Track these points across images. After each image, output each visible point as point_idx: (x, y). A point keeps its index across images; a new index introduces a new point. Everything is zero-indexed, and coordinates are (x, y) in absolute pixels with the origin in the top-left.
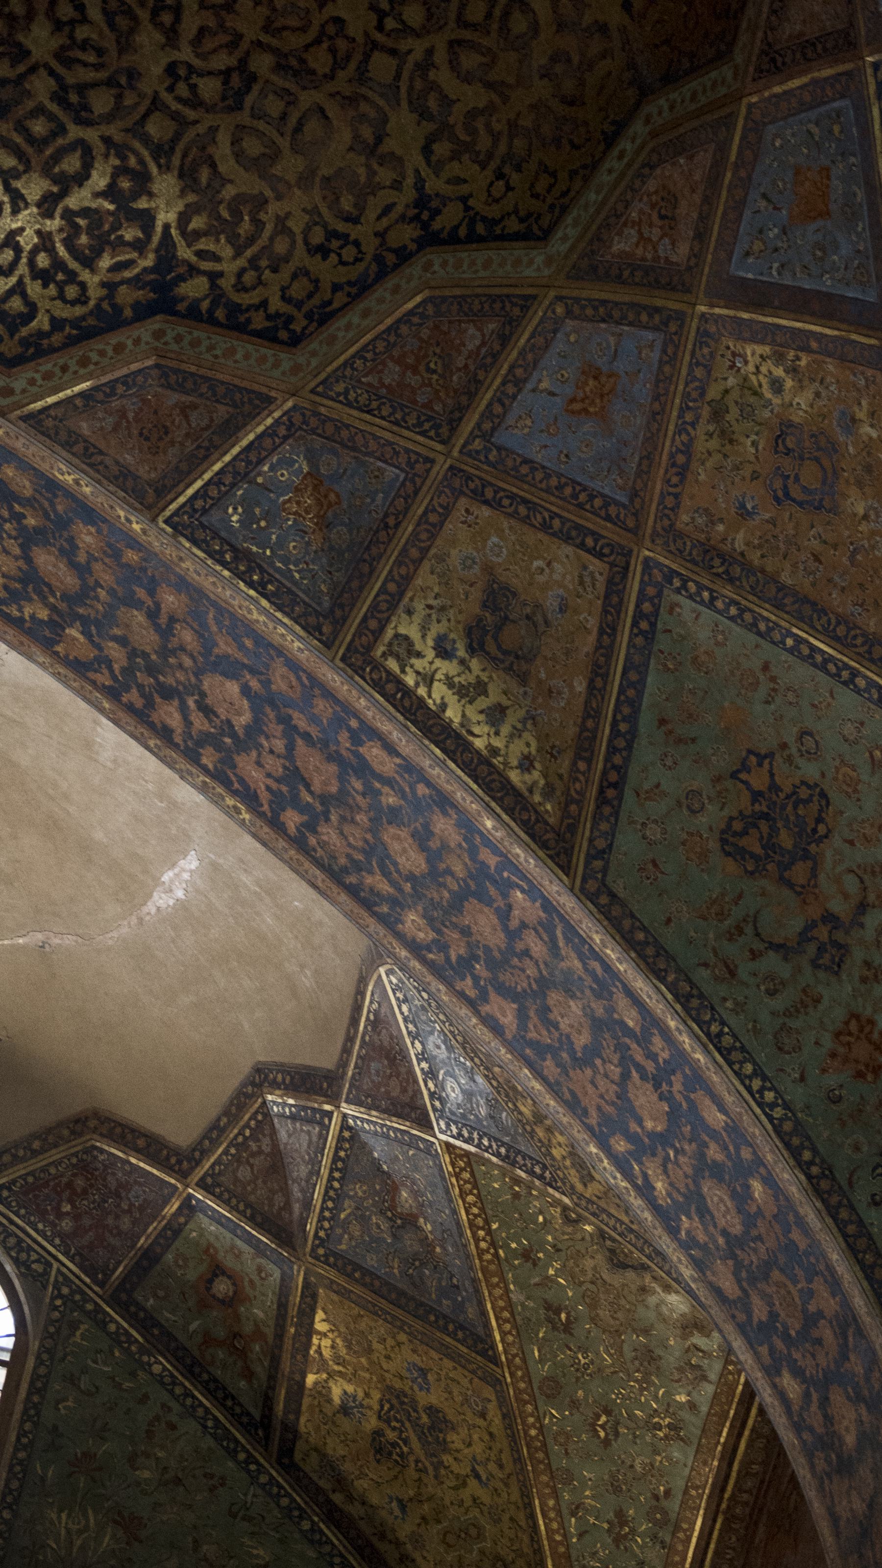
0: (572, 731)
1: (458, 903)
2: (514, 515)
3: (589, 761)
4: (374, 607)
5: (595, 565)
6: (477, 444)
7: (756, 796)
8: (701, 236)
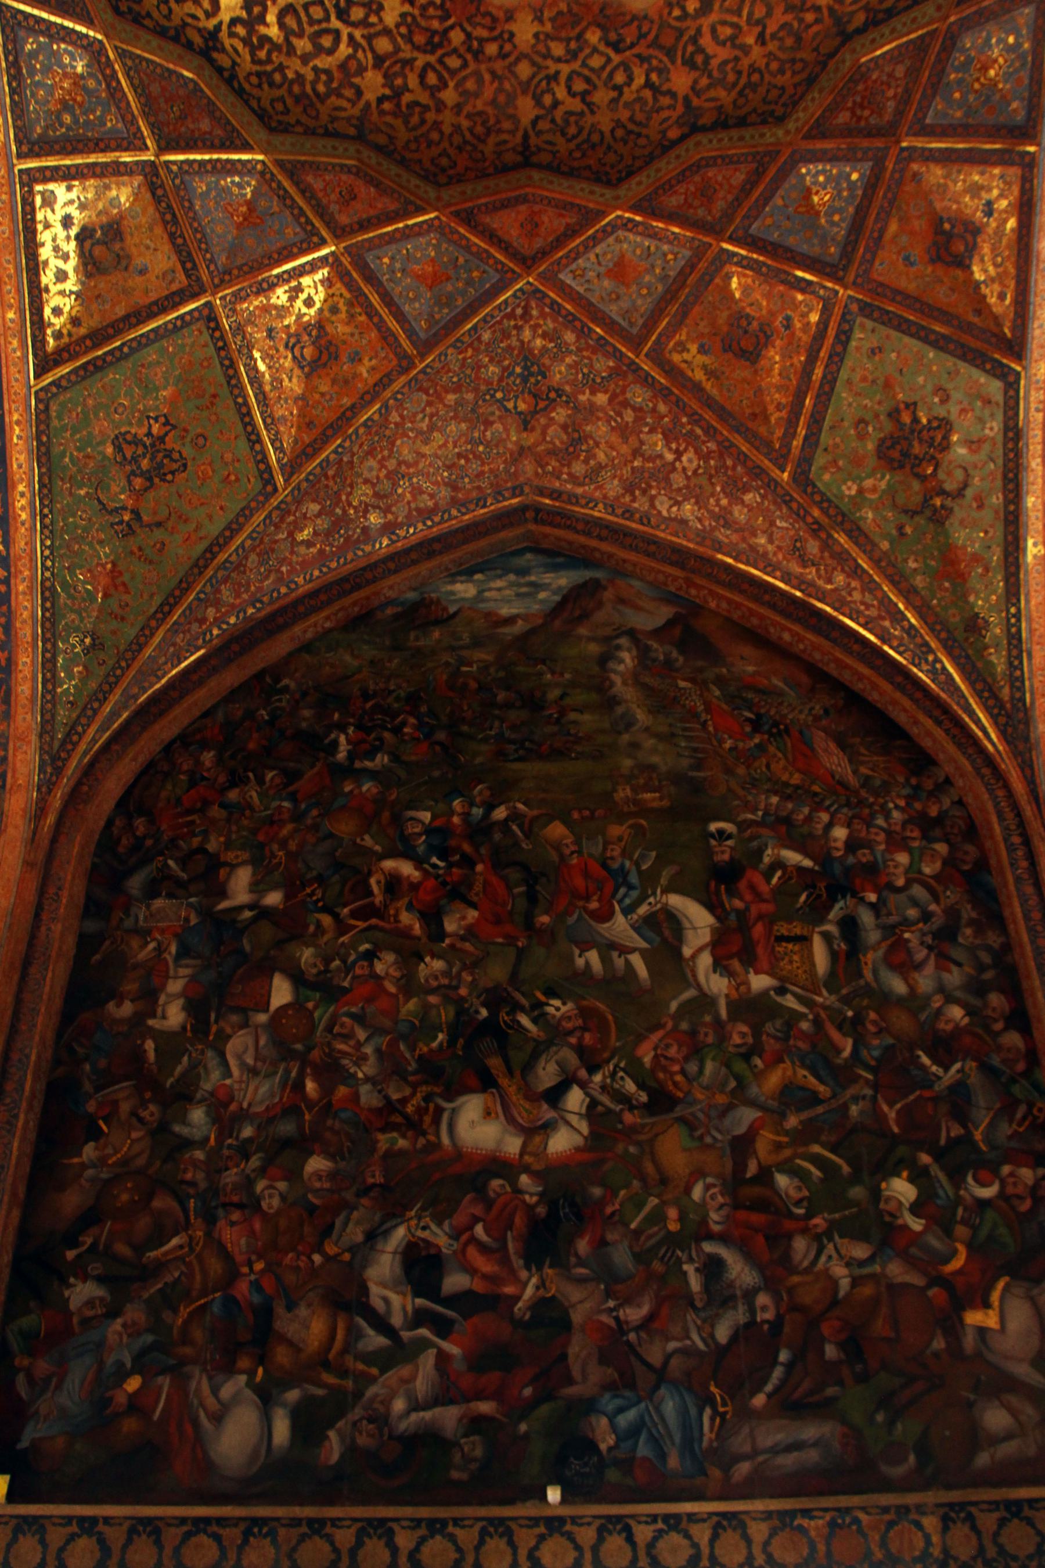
2: (163, 215)
3: (96, 346)
4: (57, 168)
5: (181, 277)
6: (174, 168)
7: (149, 434)
8: (363, 226)
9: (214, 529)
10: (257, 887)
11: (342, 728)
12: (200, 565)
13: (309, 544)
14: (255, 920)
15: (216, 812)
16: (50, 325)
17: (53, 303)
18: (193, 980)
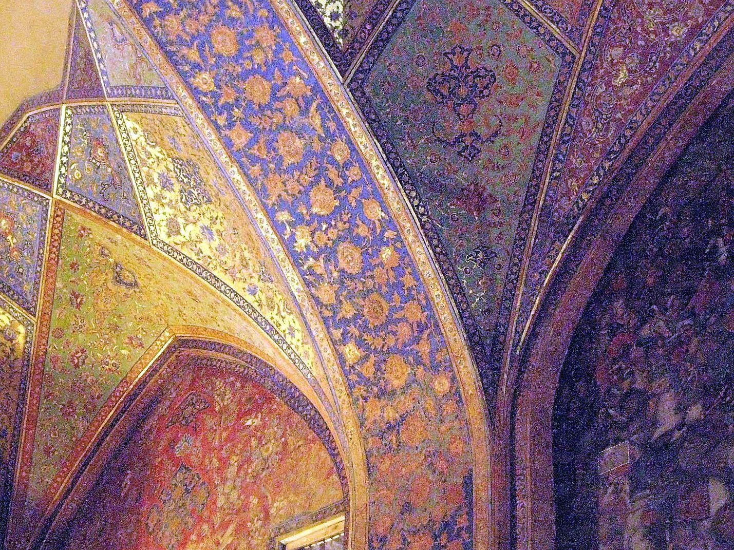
0: (366, 8)
1: (245, 76)
3: (374, 26)
7: (454, 67)
9: (539, 115)
10: (681, 409)
11: (717, 232)
12: (542, 152)
13: (630, 83)
14: (684, 438)
15: (636, 352)
16: (334, 29)
17: (328, 13)
18: (648, 512)
